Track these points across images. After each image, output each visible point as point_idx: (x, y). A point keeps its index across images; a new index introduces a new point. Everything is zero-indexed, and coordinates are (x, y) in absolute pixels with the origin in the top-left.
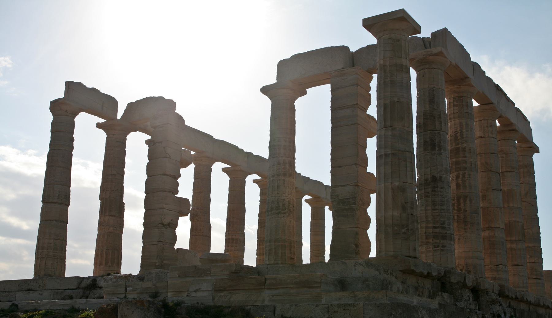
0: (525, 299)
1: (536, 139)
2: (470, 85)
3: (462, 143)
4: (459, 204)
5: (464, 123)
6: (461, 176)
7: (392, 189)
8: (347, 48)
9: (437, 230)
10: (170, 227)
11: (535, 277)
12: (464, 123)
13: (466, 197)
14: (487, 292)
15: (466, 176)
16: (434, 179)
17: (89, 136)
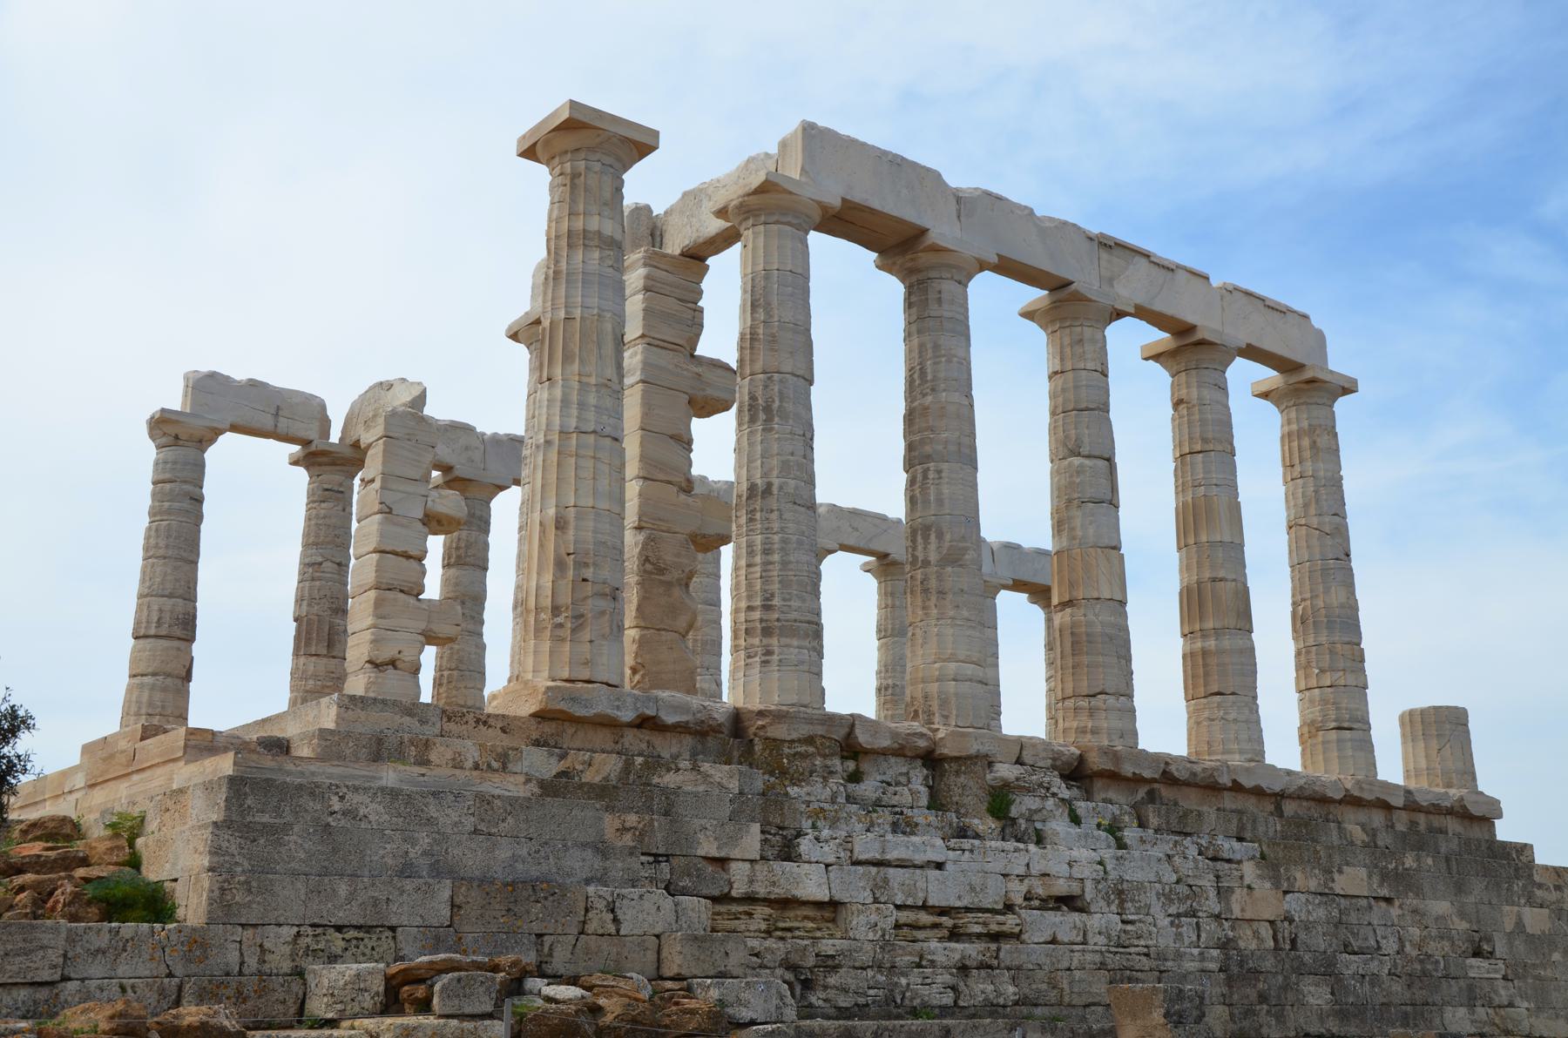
0: (1225, 780)
1: (1339, 361)
2: (936, 249)
3: (924, 395)
4: (914, 549)
5: (929, 346)
6: (919, 477)
7: (541, 524)
8: (648, 209)
9: (757, 615)
10: (395, 668)
11: (1333, 725)
12: (929, 346)
13: (926, 529)
14: (990, 764)
15: (931, 475)
16: (752, 488)
17: (256, 486)
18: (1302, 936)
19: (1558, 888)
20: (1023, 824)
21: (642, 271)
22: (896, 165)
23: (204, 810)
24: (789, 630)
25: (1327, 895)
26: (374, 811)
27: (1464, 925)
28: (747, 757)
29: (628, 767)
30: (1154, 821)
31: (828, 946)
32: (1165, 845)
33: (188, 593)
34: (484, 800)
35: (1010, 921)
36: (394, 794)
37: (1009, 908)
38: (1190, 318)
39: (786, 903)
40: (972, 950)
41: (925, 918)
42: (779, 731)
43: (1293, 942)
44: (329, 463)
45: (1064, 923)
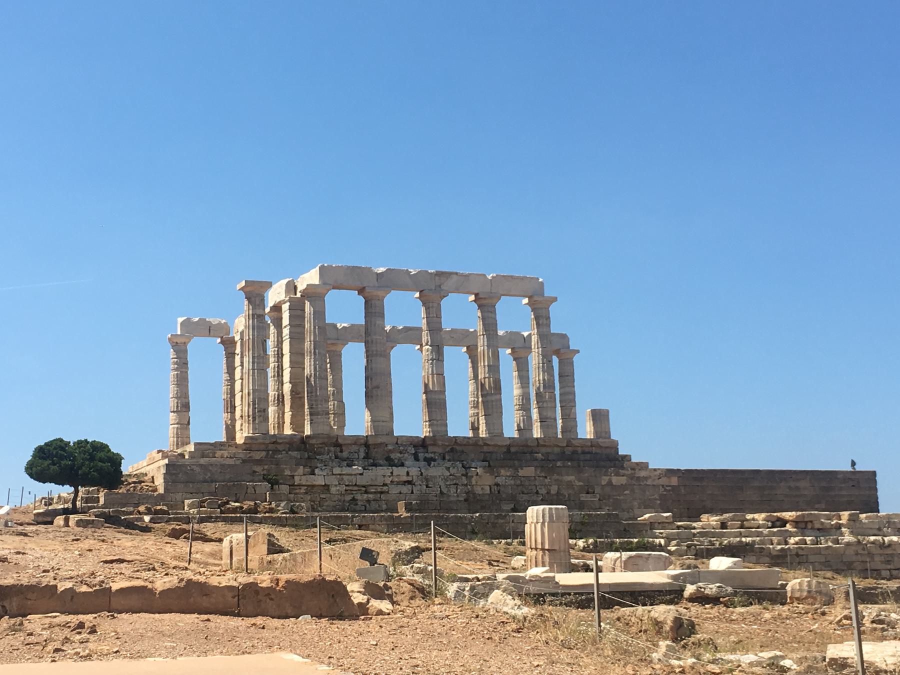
0: (481, 443)
17: (206, 355)
18: (502, 489)
19: (633, 469)
20: (396, 461)
21: (288, 304)
22: (354, 269)
23: (163, 471)
24: (318, 414)
25: (515, 477)
26: (197, 469)
27: (581, 483)
28: (305, 450)
29: (268, 454)
30: (447, 457)
31: (323, 496)
32: (448, 464)
33: (186, 396)
34: (223, 466)
35: (385, 488)
36: (201, 465)
37: (385, 485)
38: (476, 292)
39: (313, 486)
40: (371, 496)
41: (356, 488)
42: (313, 441)
43: (499, 492)
44: (228, 344)
45: (406, 489)
